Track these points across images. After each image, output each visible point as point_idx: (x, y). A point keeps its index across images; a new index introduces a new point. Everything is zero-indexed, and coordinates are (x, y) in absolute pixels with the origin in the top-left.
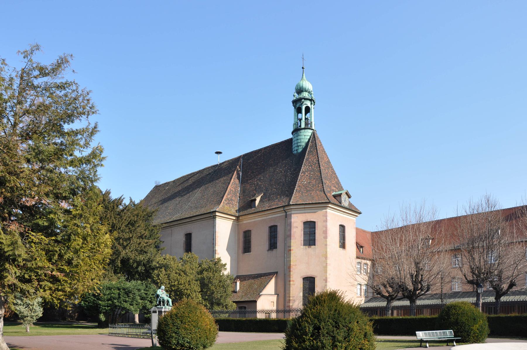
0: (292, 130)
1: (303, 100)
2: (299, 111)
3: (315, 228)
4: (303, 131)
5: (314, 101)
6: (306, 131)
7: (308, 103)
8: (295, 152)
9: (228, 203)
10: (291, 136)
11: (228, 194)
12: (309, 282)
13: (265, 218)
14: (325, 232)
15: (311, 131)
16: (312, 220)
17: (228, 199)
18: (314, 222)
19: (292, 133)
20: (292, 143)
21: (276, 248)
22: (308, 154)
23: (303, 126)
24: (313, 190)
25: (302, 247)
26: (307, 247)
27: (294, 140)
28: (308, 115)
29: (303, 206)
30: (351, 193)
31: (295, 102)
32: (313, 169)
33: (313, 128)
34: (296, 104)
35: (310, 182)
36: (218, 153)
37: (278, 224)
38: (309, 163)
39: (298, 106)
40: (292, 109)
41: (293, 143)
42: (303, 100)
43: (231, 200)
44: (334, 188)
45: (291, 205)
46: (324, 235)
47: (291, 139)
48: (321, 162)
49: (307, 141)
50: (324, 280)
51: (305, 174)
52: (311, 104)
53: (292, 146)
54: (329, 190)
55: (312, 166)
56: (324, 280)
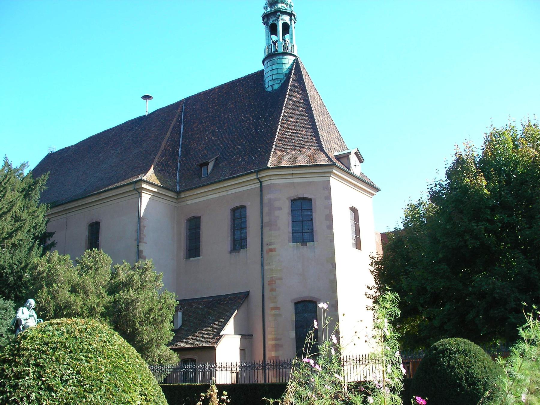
0: (263, 57)
2: (273, 29)
3: (311, 210)
5: (294, 15)
7: (287, 18)
8: (270, 89)
9: (162, 170)
10: (261, 67)
11: (162, 156)
13: (225, 193)
15: (293, 58)
16: (306, 196)
17: (162, 163)
18: (310, 200)
19: (263, 62)
20: (263, 77)
21: (245, 246)
25: (291, 244)
26: (299, 244)
27: (266, 72)
28: (287, 37)
29: (289, 172)
30: (363, 154)
31: (266, 17)
33: (295, 54)
34: (268, 20)
35: (297, 133)
37: (248, 204)
39: (271, 22)
40: (262, 29)
41: (266, 76)
42: (279, 14)
44: (336, 146)
45: (269, 168)
47: (262, 72)
48: (313, 103)
52: (291, 20)
53: (263, 80)
54: (329, 147)
55: (298, 109)
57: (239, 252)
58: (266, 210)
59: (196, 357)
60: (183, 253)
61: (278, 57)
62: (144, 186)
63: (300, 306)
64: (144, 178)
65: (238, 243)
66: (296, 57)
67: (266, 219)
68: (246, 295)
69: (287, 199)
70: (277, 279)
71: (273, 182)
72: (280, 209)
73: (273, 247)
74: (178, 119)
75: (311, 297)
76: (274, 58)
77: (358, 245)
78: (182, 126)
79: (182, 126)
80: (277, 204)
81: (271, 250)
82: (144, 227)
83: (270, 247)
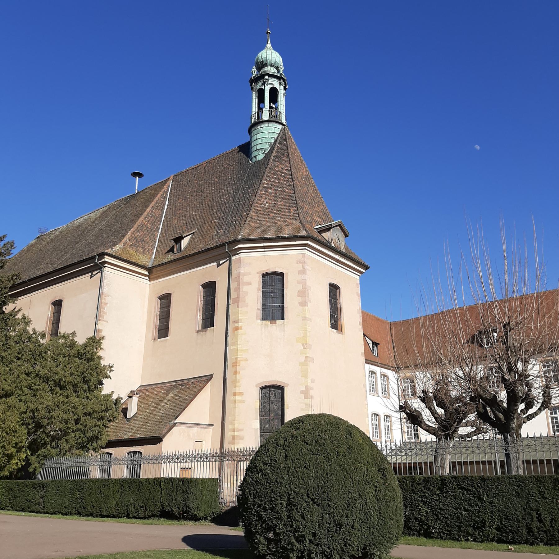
1: (266, 77)
4: (266, 125)
6: (271, 125)
11: (137, 231)
12: (273, 394)
14: (303, 293)
17: (136, 238)
18: (282, 275)
21: (212, 325)
22: (273, 160)
23: (266, 116)
24: (281, 217)
25: (260, 322)
26: (268, 322)
32: (282, 185)
33: (283, 121)
35: (275, 205)
36: (135, 174)
38: (275, 173)
42: (266, 77)
43: (142, 241)
46: (300, 299)
49: (273, 141)
50: (302, 392)
51: (266, 191)
55: (279, 179)
56: (302, 392)
57: (206, 331)
58: (233, 285)
59: (113, 452)
60: (150, 335)
61: (263, 125)
62: (107, 259)
63: (266, 391)
64: (109, 251)
65: (208, 321)
66: (283, 125)
67: (233, 295)
68: (210, 377)
69: (258, 273)
70: (242, 361)
71: (242, 255)
72: (249, 284)
73: (240, 324)
74: (163, 195)
75: (278, 381)
76: (259, 127)
77: (336, 323)
78: (167, 202)
79: (167, 202)
80: (245, 279)
81: (237, 329)
82: (106, 304)
83: (236, 325)
